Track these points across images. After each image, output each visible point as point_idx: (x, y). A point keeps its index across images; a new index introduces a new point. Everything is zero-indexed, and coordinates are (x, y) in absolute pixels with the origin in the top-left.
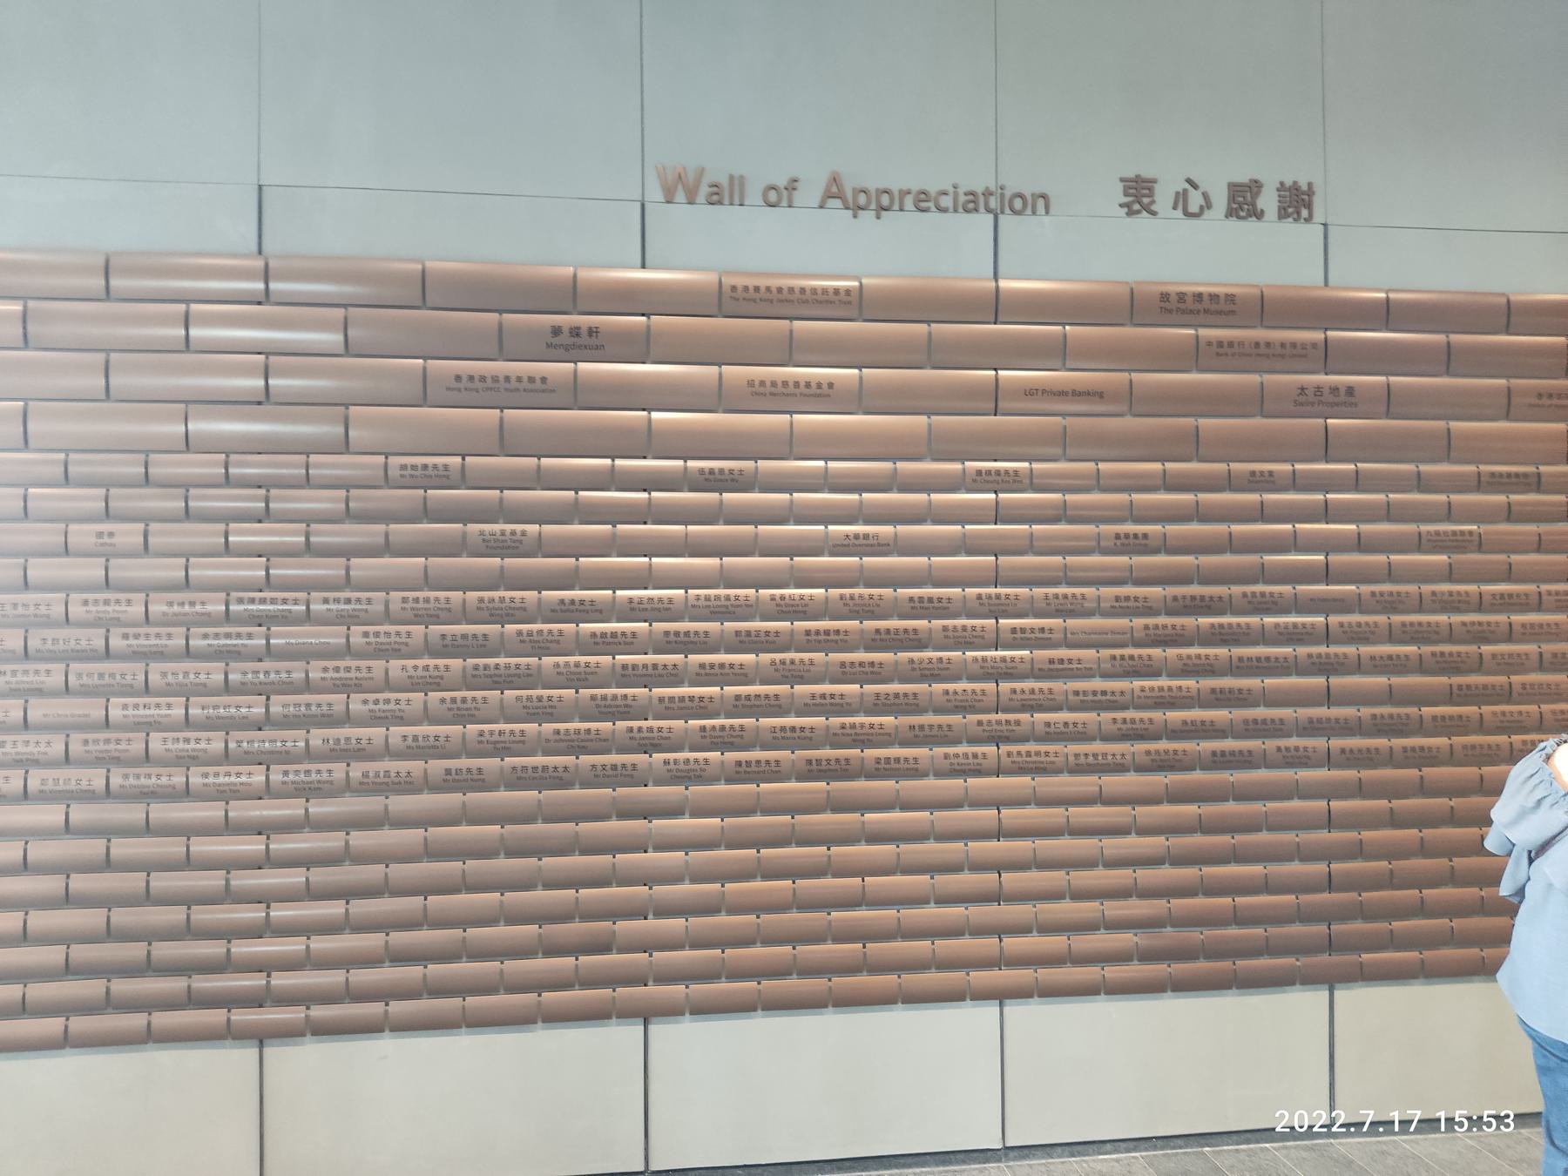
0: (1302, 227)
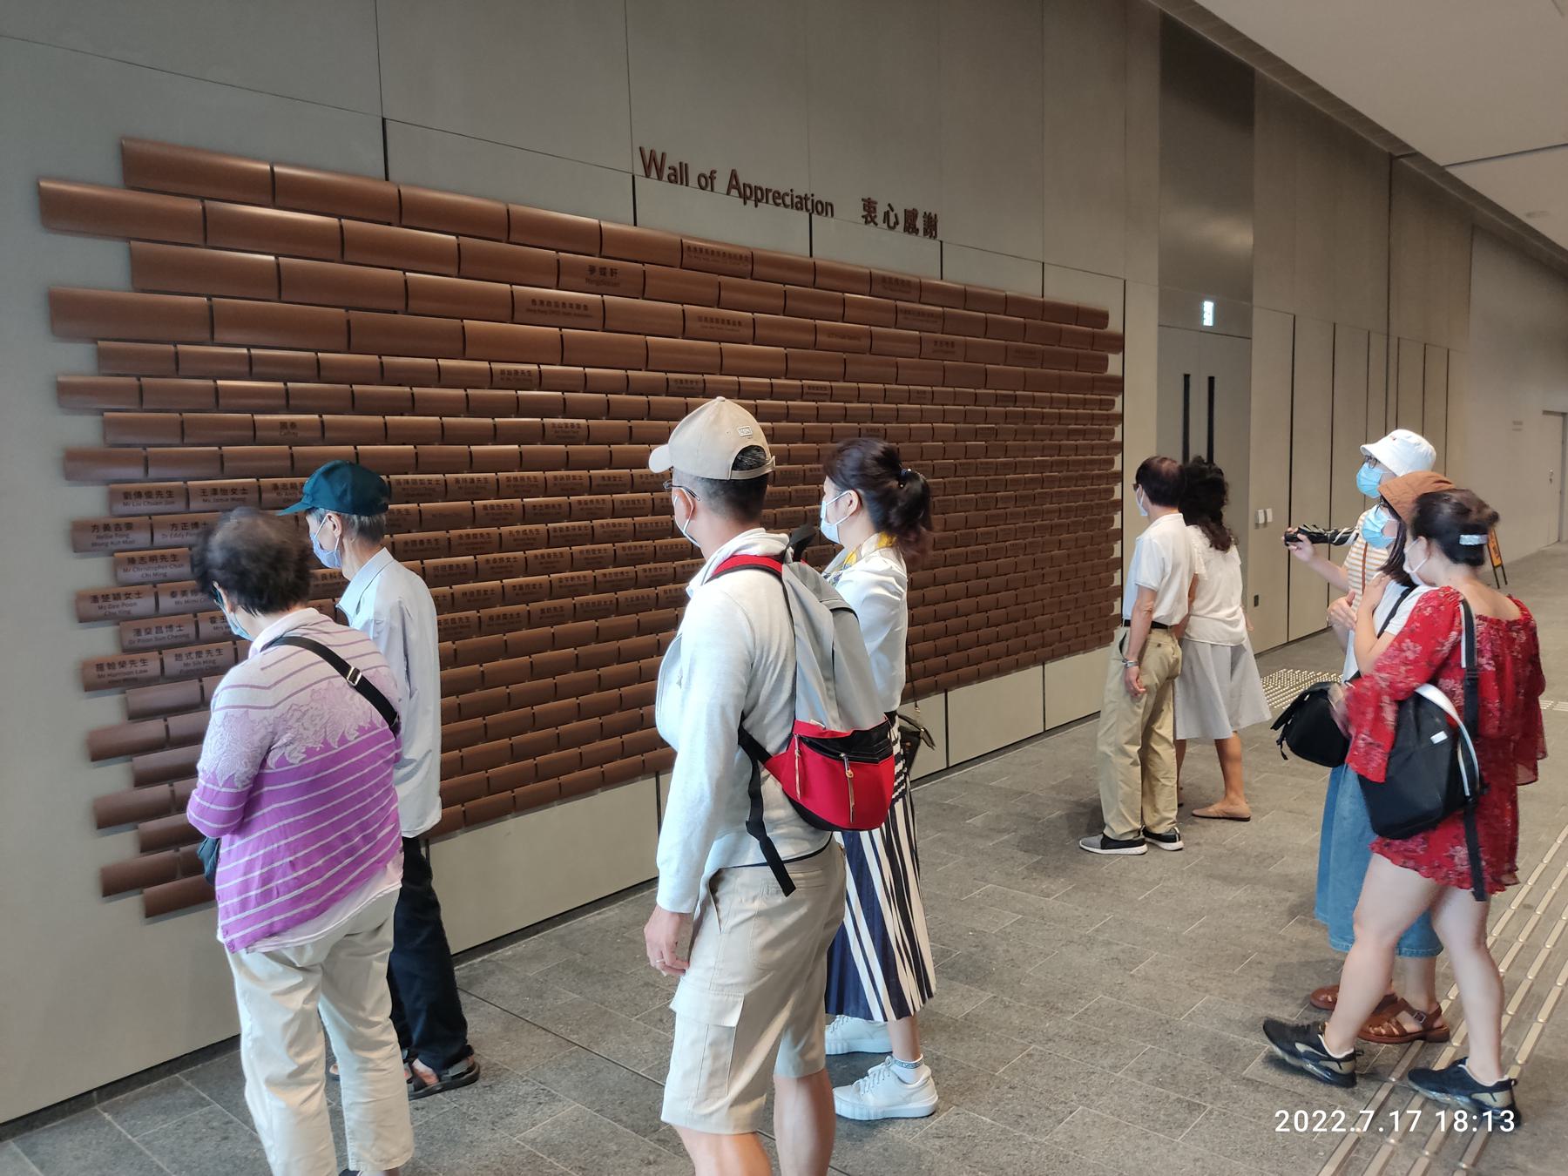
0: (932, 241)
